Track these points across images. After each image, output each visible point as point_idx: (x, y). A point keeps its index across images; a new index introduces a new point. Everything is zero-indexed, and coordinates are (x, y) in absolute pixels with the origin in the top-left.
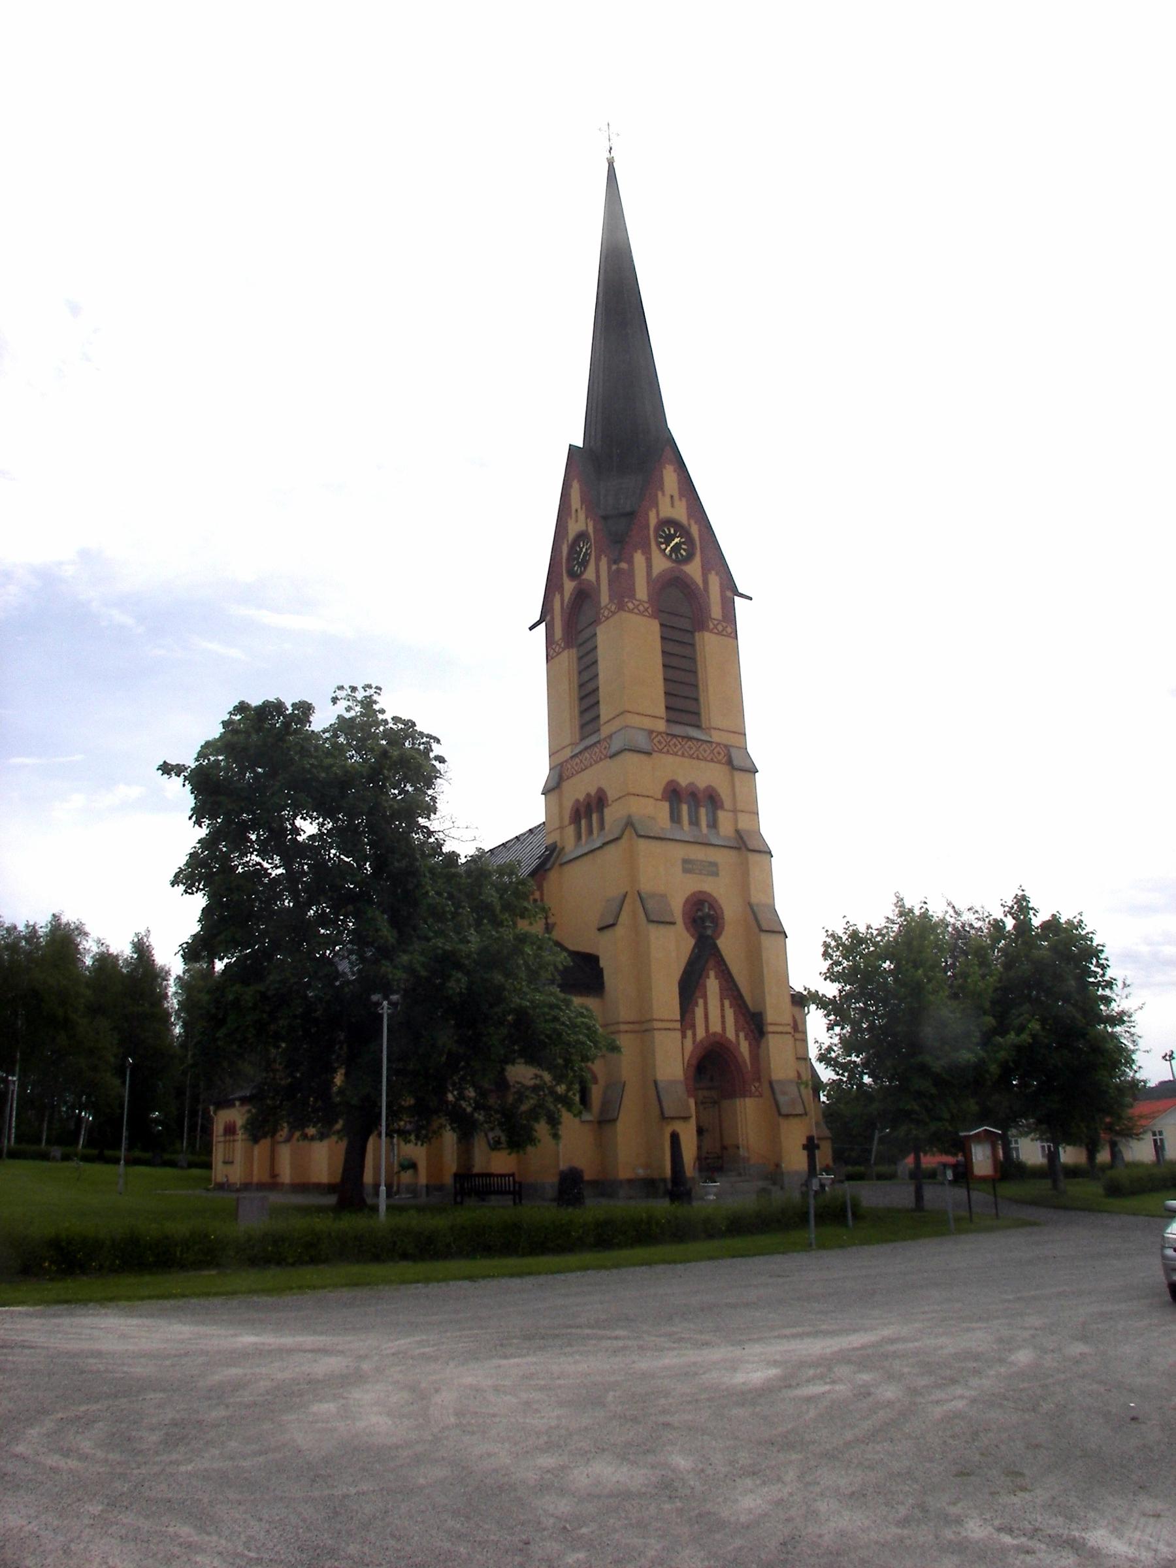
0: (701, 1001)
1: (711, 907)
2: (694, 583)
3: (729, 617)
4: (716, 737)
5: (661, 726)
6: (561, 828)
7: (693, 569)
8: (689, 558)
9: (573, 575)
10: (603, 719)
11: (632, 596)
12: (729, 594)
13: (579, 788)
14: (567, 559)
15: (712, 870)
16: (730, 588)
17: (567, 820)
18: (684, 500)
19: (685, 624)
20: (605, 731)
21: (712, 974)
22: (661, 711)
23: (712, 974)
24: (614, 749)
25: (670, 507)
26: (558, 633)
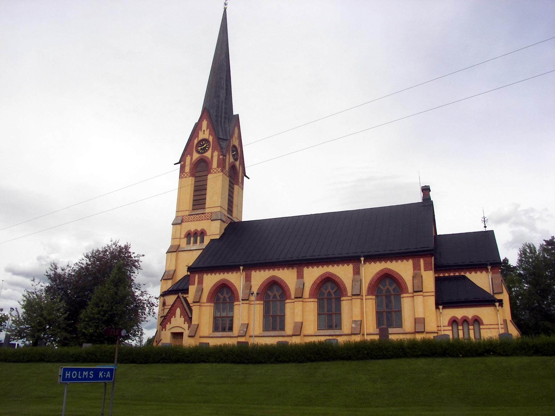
17: (183, 236)
18: (208, 130)
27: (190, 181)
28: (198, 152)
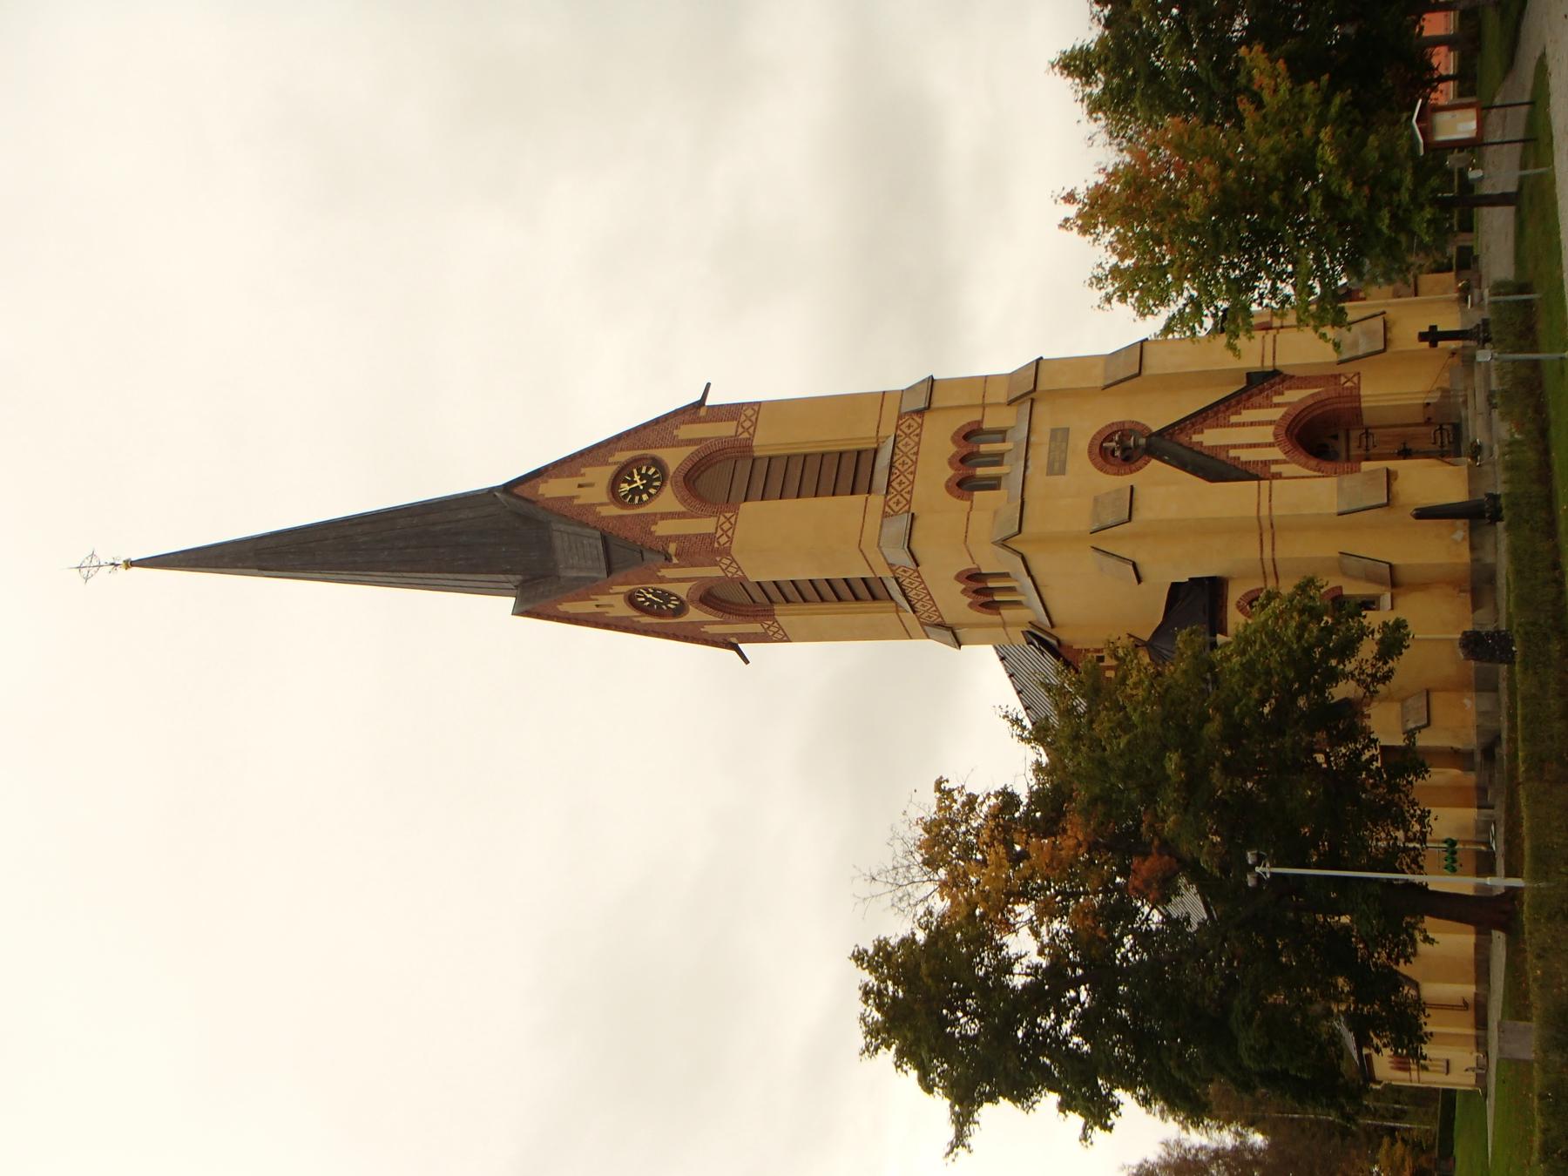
0: (1233, 453)
1: (1109, 438)
3: (732, 412)
4: (888, 430)
5: (876, 500)
7: (674, 458)
8: (656, 462)
9: (681, 610)
10: (868, 575)
11: (711, 537)
12: (703, 412)
13: (954, 602)
14: (657, 617)
15: (1060, 436)
16: (695, 411)
18: (583, 470)
19: (743, 469)
20: (886, 574)
21: (1196, 438)
22: (859, 499)
23: (1196, 438)
24: (911, 565)
25: (593, 490)
26: (756, 627)
27: (785, 616)
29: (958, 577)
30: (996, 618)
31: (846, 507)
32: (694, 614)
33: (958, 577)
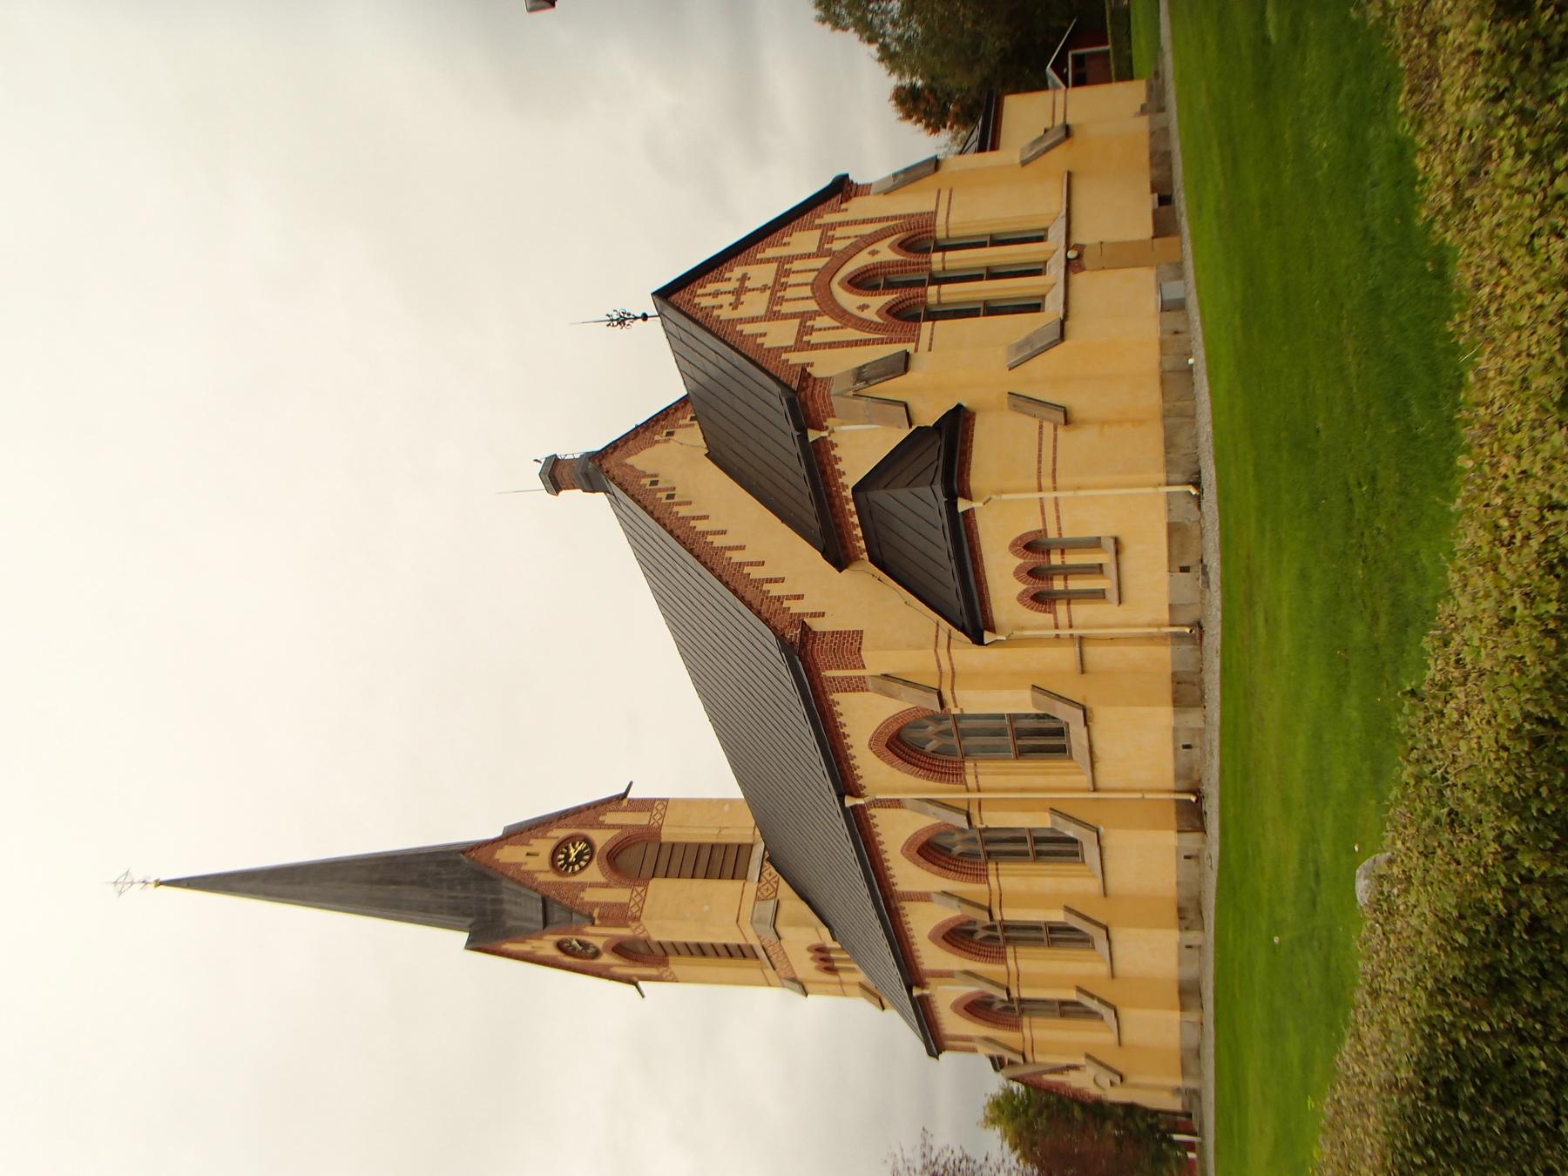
2: (615, 837)
3: (646, 805)
5: (751, 887)
6: (841, 983)
7: (601, 838)
8: (587, 840)
9: (597, 954)
10: (741, 942)
12: (625, 803)
14: (577, 959)
16: (618, 801)
19: (652, 850)
20: (756, 943)
22: (738, 884)
26: (652, 971)
28: (582, 868)
29: (809, 949)
30: (834, 978)
31: (726, 890)
32: (606, 959)
33: (809, 949)
